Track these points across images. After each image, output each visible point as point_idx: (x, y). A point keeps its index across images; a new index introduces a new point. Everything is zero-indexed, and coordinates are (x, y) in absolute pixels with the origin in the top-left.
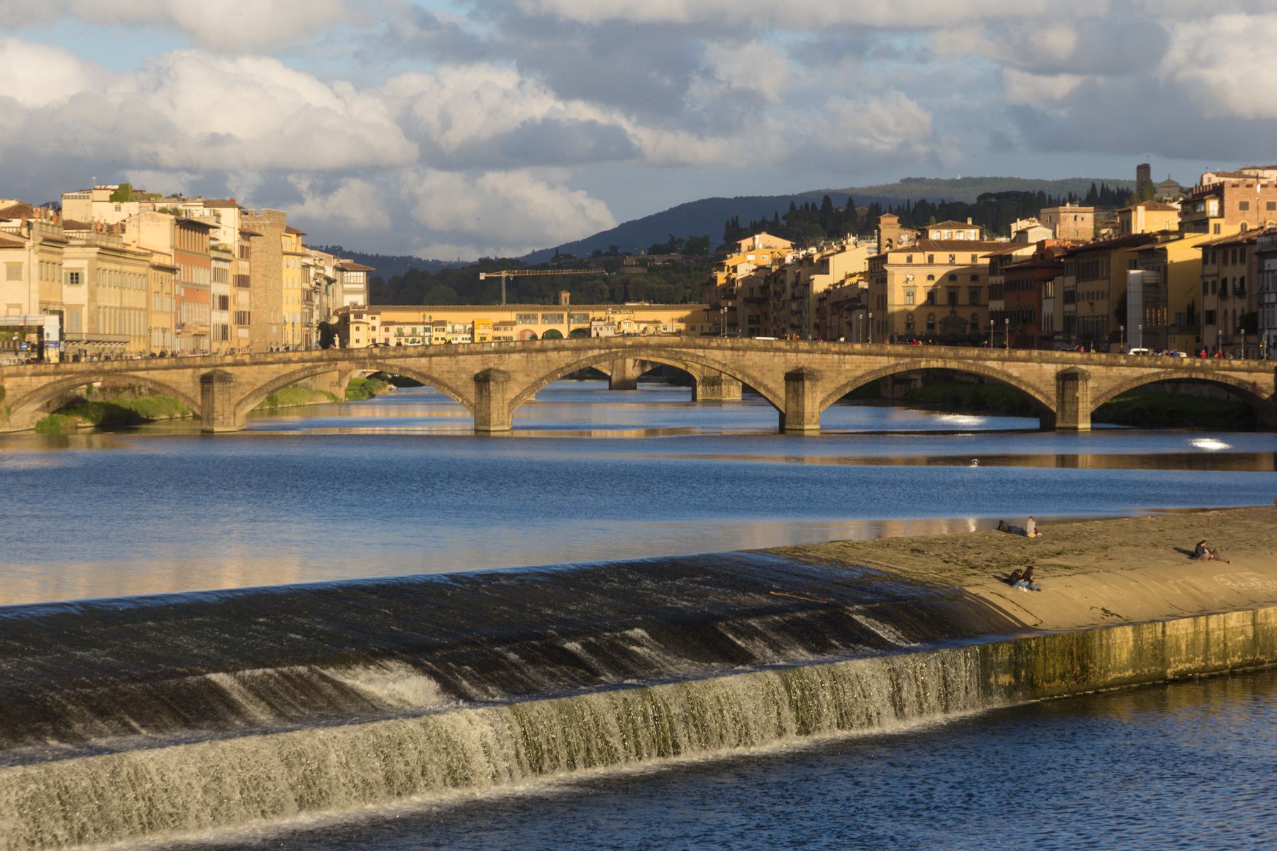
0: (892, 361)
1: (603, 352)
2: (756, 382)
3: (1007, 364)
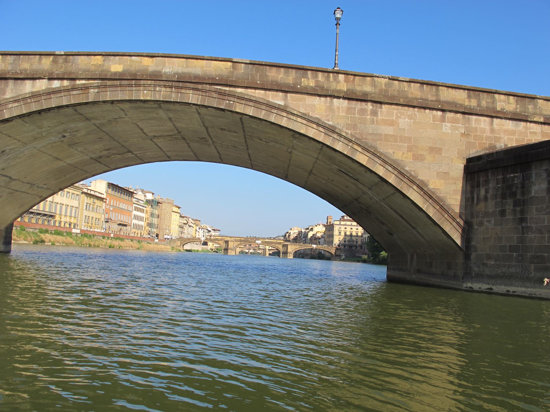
1: (56, 84)
2: (402, 174)
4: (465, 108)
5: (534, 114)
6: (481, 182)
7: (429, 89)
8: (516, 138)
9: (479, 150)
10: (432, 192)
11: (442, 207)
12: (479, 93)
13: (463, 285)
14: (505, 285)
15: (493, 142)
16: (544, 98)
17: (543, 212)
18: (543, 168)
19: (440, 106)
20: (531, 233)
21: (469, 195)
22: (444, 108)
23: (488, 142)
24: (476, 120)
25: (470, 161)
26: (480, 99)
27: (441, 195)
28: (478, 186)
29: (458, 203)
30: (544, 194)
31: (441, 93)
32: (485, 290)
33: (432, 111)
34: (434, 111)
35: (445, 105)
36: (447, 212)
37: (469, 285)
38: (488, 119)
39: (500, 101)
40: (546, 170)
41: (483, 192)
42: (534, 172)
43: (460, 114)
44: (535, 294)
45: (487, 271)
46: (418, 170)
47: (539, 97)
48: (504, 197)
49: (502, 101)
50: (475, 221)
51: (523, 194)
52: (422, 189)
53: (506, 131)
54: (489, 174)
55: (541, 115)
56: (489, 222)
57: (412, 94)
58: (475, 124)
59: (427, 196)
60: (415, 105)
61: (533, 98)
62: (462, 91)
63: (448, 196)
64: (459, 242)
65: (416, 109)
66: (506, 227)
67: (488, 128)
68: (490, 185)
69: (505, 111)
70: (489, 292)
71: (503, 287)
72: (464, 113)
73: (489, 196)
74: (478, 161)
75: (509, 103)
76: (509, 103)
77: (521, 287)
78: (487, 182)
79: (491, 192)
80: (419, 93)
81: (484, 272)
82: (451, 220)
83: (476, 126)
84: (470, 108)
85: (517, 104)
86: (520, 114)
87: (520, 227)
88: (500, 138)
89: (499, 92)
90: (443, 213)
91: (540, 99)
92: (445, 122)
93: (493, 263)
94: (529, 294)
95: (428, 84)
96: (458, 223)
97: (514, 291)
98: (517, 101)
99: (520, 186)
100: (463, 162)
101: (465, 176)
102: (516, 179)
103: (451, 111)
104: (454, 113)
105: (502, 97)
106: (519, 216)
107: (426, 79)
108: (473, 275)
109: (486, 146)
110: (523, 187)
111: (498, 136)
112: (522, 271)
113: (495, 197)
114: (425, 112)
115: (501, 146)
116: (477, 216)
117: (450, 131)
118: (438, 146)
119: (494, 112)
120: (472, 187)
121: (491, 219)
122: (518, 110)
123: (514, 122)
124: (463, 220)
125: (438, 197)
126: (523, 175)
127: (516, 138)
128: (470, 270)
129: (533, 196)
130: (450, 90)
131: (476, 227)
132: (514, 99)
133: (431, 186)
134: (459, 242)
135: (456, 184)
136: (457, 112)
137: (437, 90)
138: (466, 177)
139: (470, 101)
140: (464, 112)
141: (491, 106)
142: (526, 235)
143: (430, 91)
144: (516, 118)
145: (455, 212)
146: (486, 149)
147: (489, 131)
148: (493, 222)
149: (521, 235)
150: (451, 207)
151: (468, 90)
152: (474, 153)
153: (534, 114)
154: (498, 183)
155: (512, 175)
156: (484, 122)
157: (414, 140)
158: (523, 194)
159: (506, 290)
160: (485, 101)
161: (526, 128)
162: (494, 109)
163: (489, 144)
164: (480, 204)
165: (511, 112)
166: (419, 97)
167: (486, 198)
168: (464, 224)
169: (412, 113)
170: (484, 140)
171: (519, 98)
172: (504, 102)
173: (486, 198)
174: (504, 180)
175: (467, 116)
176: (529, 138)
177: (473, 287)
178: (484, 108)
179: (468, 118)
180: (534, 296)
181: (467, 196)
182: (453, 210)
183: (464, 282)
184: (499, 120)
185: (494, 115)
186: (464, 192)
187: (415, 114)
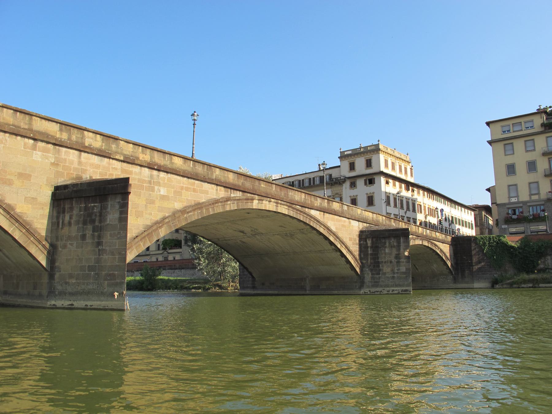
0: (221, 193)
3: (327, 215)
4: (56, 139)
5: (117, 153)
6: (66, 209)
7: (22, 117)
8: (100, 172)
9: (67, 179)
10: (19, 216)
11: (28, 230)
12: (70, 127)
13: (47, 303)
14: (84, 301)
15: (80, 173)
16: (125, 140)
17: (116, 238)
18: (117, 201)
19: (32, 135)
20: (105, 255)
21: (55, 220)
22: (36, 138)
23: (75, 173)
24: (66, 152)
25: (57, 188)
26: (71, 134)
27: (28, 219)
28: (64, 212)
29: (45, 227)
30: (117, 222)
31: (34, 123)
32: (66, 306)
33: (23, 139)
34: (26, 139)
35: (37, 134)
36: (33, 235)
37: (53, 302)
38: (77, 152)
39: (88, 137)
40: (119, 202)
41: (67, 218)
42: (110, 203)
43: (51, 145)
44: (107, 306)
45: (69, 289)
46: (5, 194)
47: (120, 139)
48: (85, 223)
49: (90, 138)
50: (59, 244)
51: (100, 221)
52: (8, 213)
53: (92, 165)
54: (74, 202)
55: (121, 154)
56: (71, 244)
57: (4, 119)
58: (65, 156)
59: (13, 219)
60: (6, 130)
61: (116, 139)
62: (54, 123)
63: (35, 220)
64: (44, 263)
65: (7, 135)
66: (86, 249)
67: (76, 160)
68: (74, 212)
69: (92, 147)
70: (71, 308)
71: (82, 302)
72: (54, 144)
73: (72, 221)
74: (65, 189)
75: (96, 140)
76: (96, 140)
77: (97, 301)
78: (71, 209)
79: (74, 218)
80: (12, 120)
81: (66, 290)
82: (37, 243)
83: (66, 157)
84: (61, 141)
85: (103, 142)
86: (105, 151)
87: (97, 250)
88: (86, 170)
89: (88, 130)
90: (29, 236)
91: (121, 140)
92: (36, 150)
93: (74, 281)
94: (103, 307)
95: (21, 112)
96: (44, 246)
97: (91, 305)
98: (103, 140)
99: (98, 214)
100: (51, 189)
101: (52, 202)
102: (95, 208)
103: (42, 141)
104: (45, 143)
105: (91, 134)
106: (96, 240)
107: (20, 107)
108: (57, 293)
109: (73, 176)
110: (101, 215)
111: (85, 168)
112: (98, 287)
113: (77, 222)
114: (16, 139)
115: (87, 178)
116: (61, 239)
117: (40, 160)
118: (27, 172)
119: (82, 147)
120: (58, 213)
121: (73, 242)
122: (103, 148)
123: (100, 157)
124: (48, 242)
125: (24, 221)
126: (101, 205)
127: (100, 172)
128: (54, 289)
129: (108, 224)
130: (43, 121)
131: (60, 249)
132: (101, 137)
133: (18, 210)
134: (44, 263)
135: (43, 209)
136: (48, 143)
137: (31, 119)
138: (53, 203)
139: (61, 134)
140: (55, 143)
141: (80, 141)
142: (101, 256)
143: (23, 119)
144: (101, 154)
145: (41, 236)
146: (73, 179)
147: (77, 163)
148: (75, 245)
149: (98, 257)
150: (37, 231)
151: (60, 123)
152: (61, 181)
153: (117, 153)
154: (80, 211)
155: (92, 205)
156: (73, 154)
157: (3, 164)
158: (100, 221)
159: (85, 305)
160: (75, 136)
161: (109, 164)
162: (83, 144)
163: (76, 174)
164: (65, 228)
165: (97, 149)
166: (11, 123)
167: (70, 224)
168: (49, 246)
169: (3, 138)
170: (72, 171)
171: (105, 137)
172: (92, 139)
173: (70, 224)
174: (86, 208)
175: (57, 147)
176: (111, 172)
177: (56, 304)
178: (74, 142)
179: (59, 149)
180: (107, 308)
181: (53, 221)
182: (39, 234)
183: (48, 300)
184: (86, 154)
185: (82, 149)
186: (51, 217)
187: (6, 139)
